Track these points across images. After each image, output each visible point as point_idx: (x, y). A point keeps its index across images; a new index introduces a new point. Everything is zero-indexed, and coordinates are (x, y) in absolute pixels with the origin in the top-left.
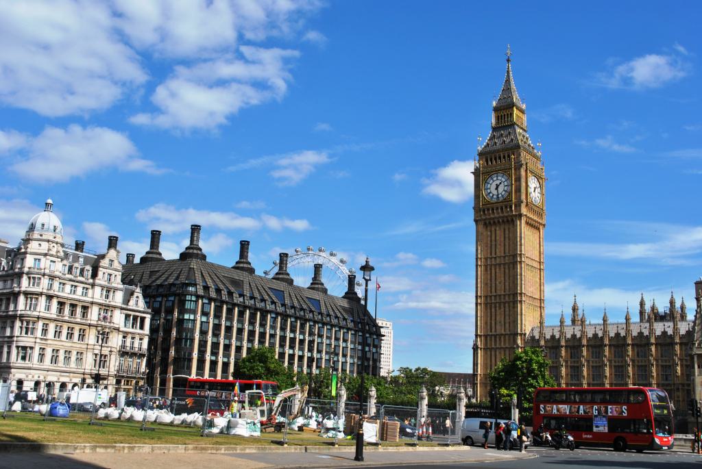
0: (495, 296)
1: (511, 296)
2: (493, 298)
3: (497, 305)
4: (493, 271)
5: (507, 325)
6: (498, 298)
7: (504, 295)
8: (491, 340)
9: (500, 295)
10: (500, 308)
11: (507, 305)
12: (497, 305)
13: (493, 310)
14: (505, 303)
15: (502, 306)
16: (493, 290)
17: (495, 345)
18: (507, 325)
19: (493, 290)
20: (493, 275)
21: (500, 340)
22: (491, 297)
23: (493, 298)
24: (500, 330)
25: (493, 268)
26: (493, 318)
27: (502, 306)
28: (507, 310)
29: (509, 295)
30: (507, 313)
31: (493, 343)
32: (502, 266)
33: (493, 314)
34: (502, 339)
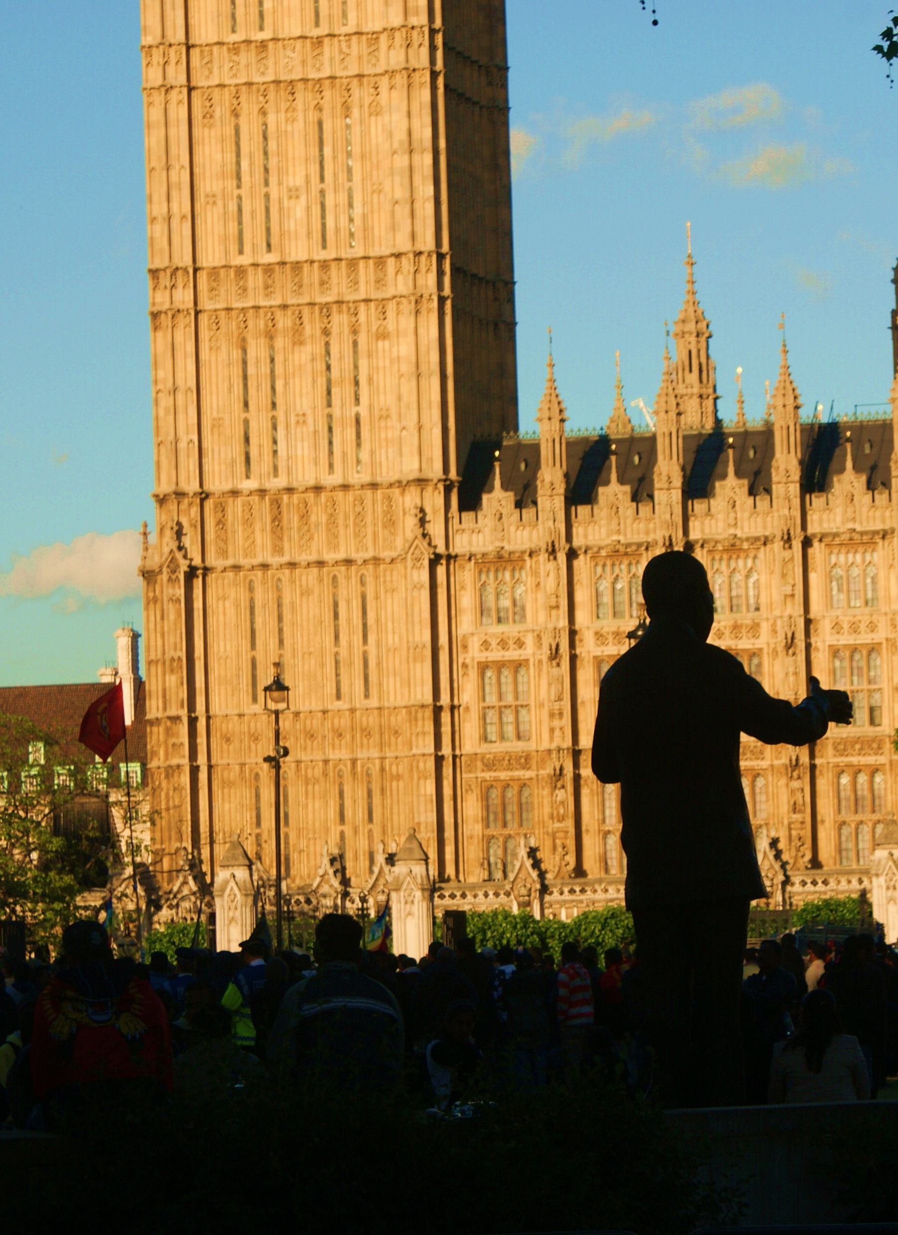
0: (268, 269)
1: (365, 272)
2: (255, 280)
3: (284, 321)
4: (250, 126)
5: (344, 436)
6: (284, 278)
7: (325, 265)
8: (248, 523)
9: (297, 266)
10: (298, 338)
11: (340, 321)
12: (284, 321)
13: (257, 350)
14: (326, 310)
15: (312, 327)
16: (254, 233)
17: (278, 550)
18: (344, 436)
19: (254, 233)
20: (250, 144)
21: (304, 517)
22: (241, 271)
23: (255, 280)
24: (303, 464)
25: (249, 106)
26: (259, 397)
27: (312, 327)
28: (340, 347)
29: (353, 263)
30: (341, 368)
31: (262, 538)
32: (304, 97)
33: (258, 371)
34: (319, 516)
